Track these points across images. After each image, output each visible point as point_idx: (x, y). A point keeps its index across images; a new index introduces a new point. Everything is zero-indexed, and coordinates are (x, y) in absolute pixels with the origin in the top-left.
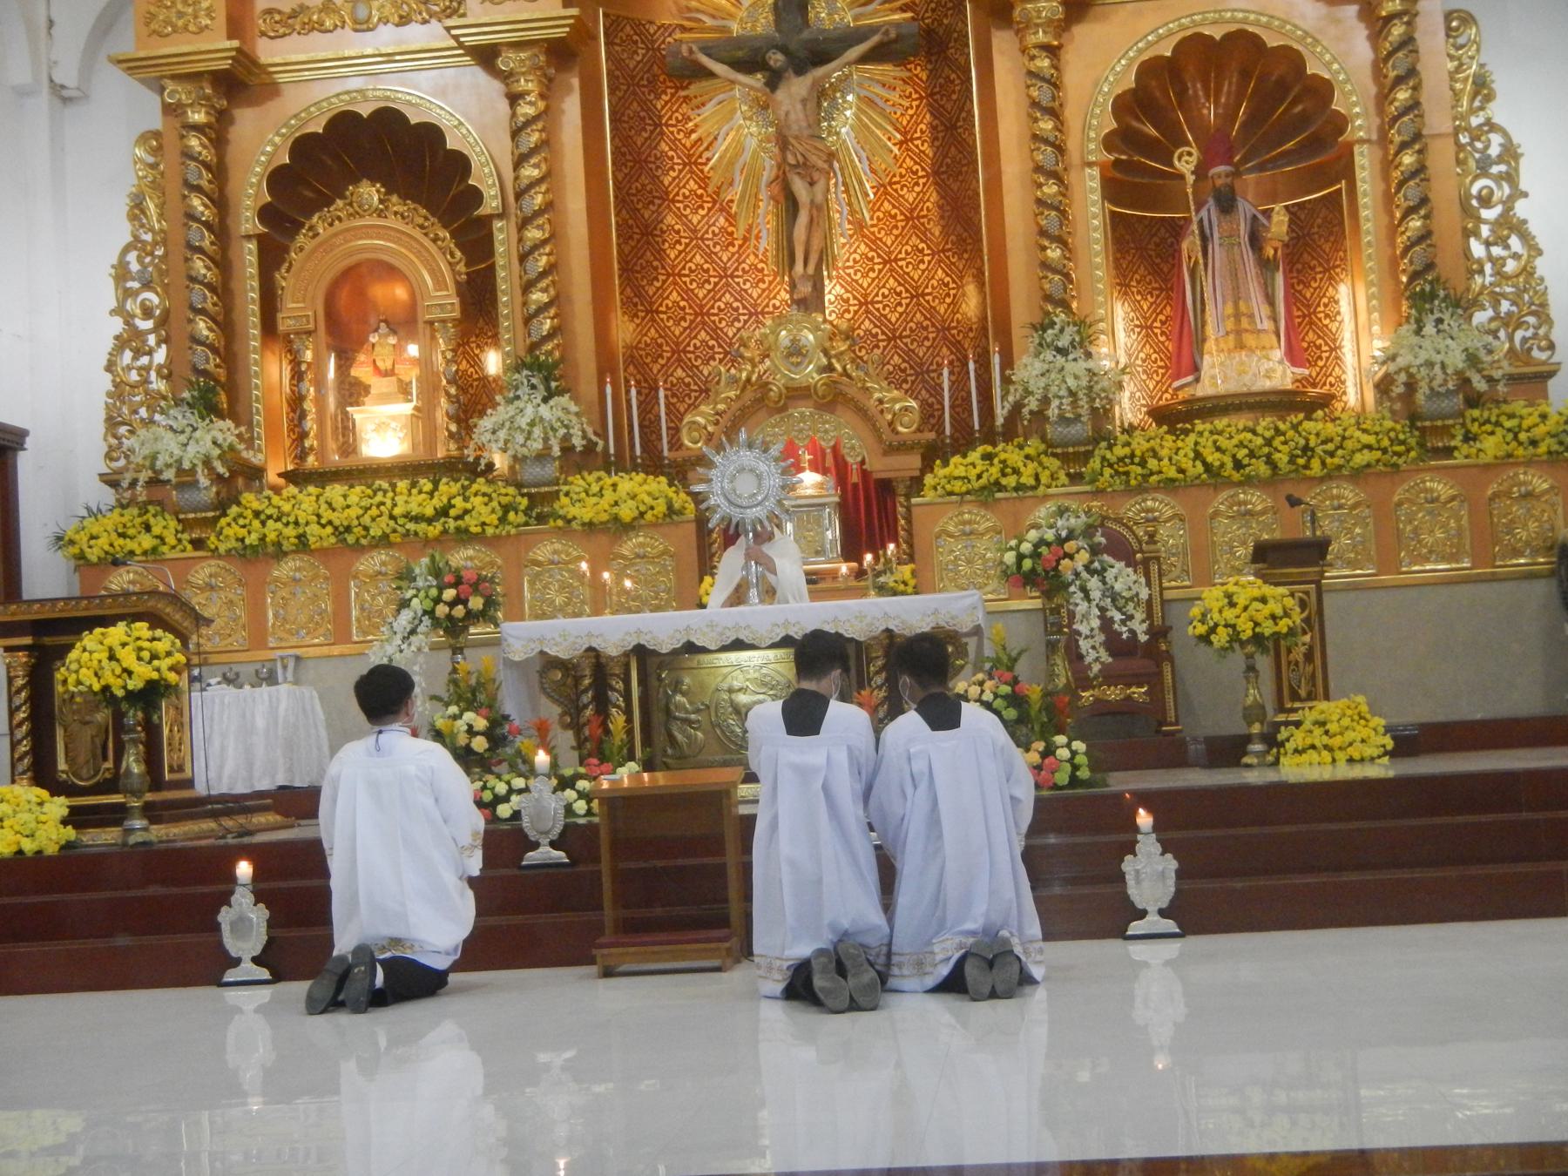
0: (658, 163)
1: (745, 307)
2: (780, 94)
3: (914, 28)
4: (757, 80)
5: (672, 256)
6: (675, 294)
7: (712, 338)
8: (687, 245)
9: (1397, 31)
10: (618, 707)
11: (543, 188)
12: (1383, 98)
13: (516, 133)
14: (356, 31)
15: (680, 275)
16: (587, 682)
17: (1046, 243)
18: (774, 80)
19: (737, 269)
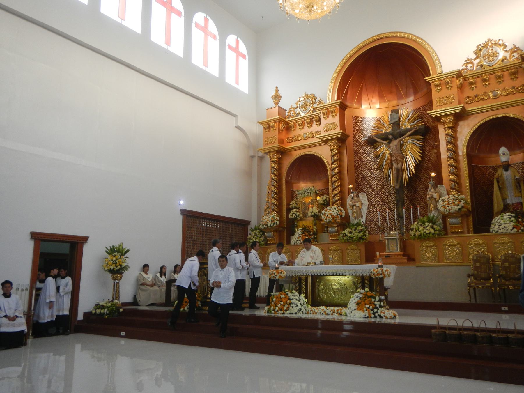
0: (367, 162)
1: (388, 192)
2: (391, 145)
3: (423, 126)
4: (386, 142)
5: (370, 182)
6: (371, 190)
7: (380, 200)
8: (374, 179)
10: (303, 288)
11: (337, 169)
13: (331, 158)
14: (304, 140)
15: (372, 186)
16: (297, 281)
17: (450, 175)
18: (390, 141)
19: (386, 184)
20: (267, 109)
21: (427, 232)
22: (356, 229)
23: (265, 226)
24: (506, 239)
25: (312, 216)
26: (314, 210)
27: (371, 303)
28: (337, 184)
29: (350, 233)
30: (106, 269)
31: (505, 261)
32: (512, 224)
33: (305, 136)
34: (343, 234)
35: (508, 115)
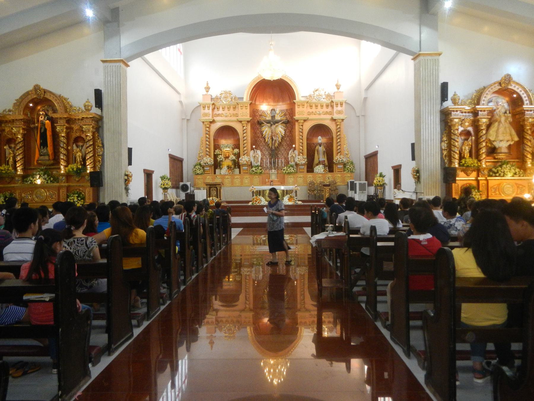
2: (272, 127)
3: (287, 120)
4: (269, 125)
9: (338, 126)
12: (337, 133)
13: (243, 131)
18: (271, 125)
20: (203, 95)
21: (292, 171)
22: (258, 169)
23: (206, 164)
24: (320, 175)
25: (232, 160)
26: (232, 157)
27: (293, 199)
28: (246, 145)
29: (256, 170)
30: (163, 187)
31: (320, 184)
32: (323, 170)
33: (226, 115)
34: (252, 170)
35: (324, 124)
